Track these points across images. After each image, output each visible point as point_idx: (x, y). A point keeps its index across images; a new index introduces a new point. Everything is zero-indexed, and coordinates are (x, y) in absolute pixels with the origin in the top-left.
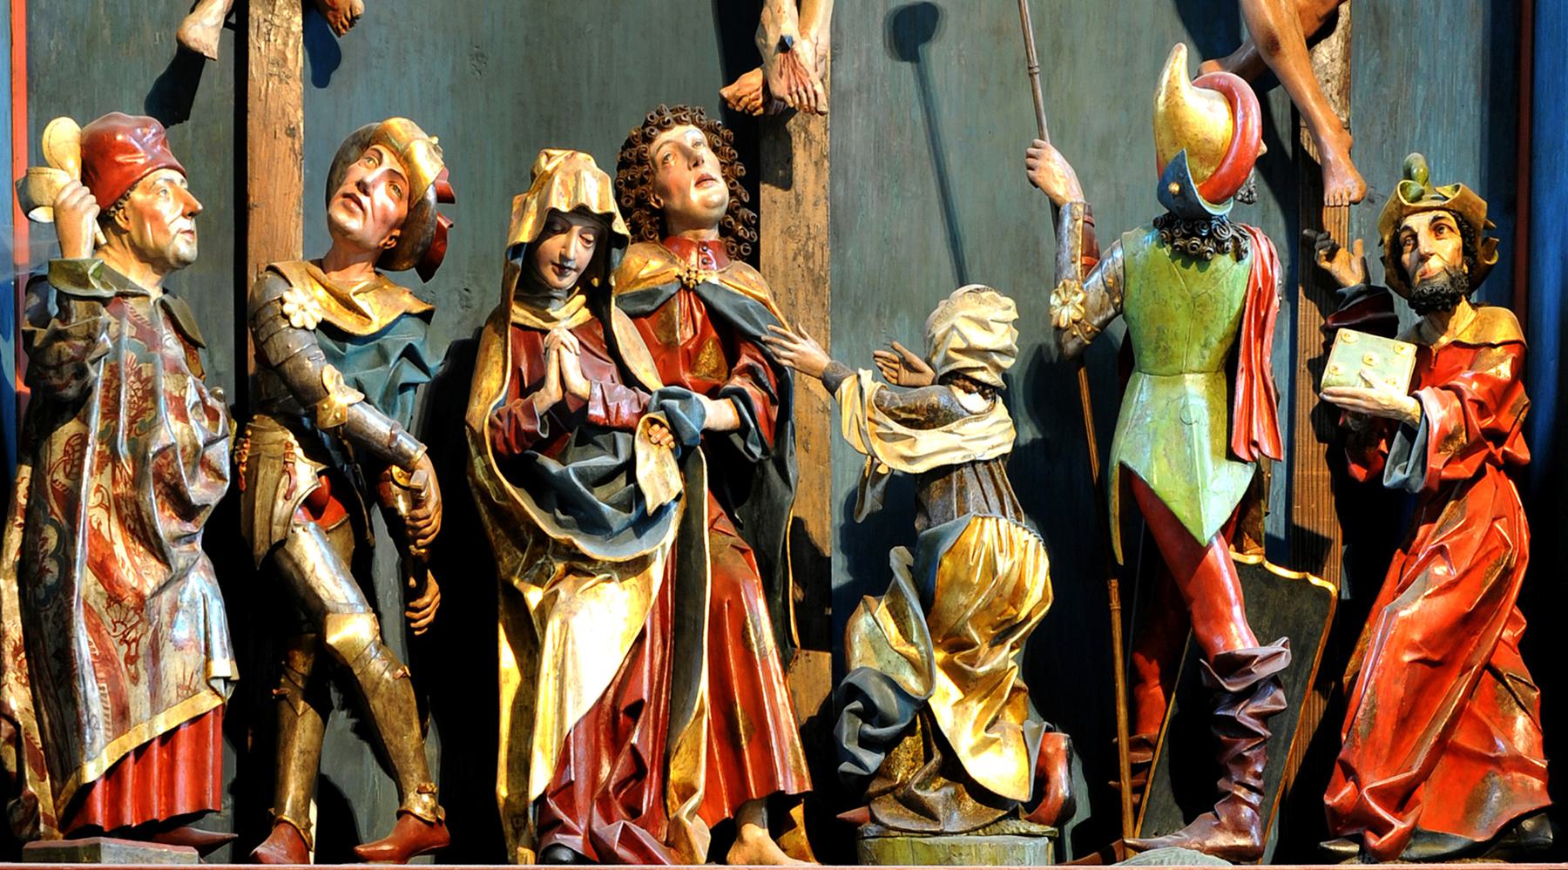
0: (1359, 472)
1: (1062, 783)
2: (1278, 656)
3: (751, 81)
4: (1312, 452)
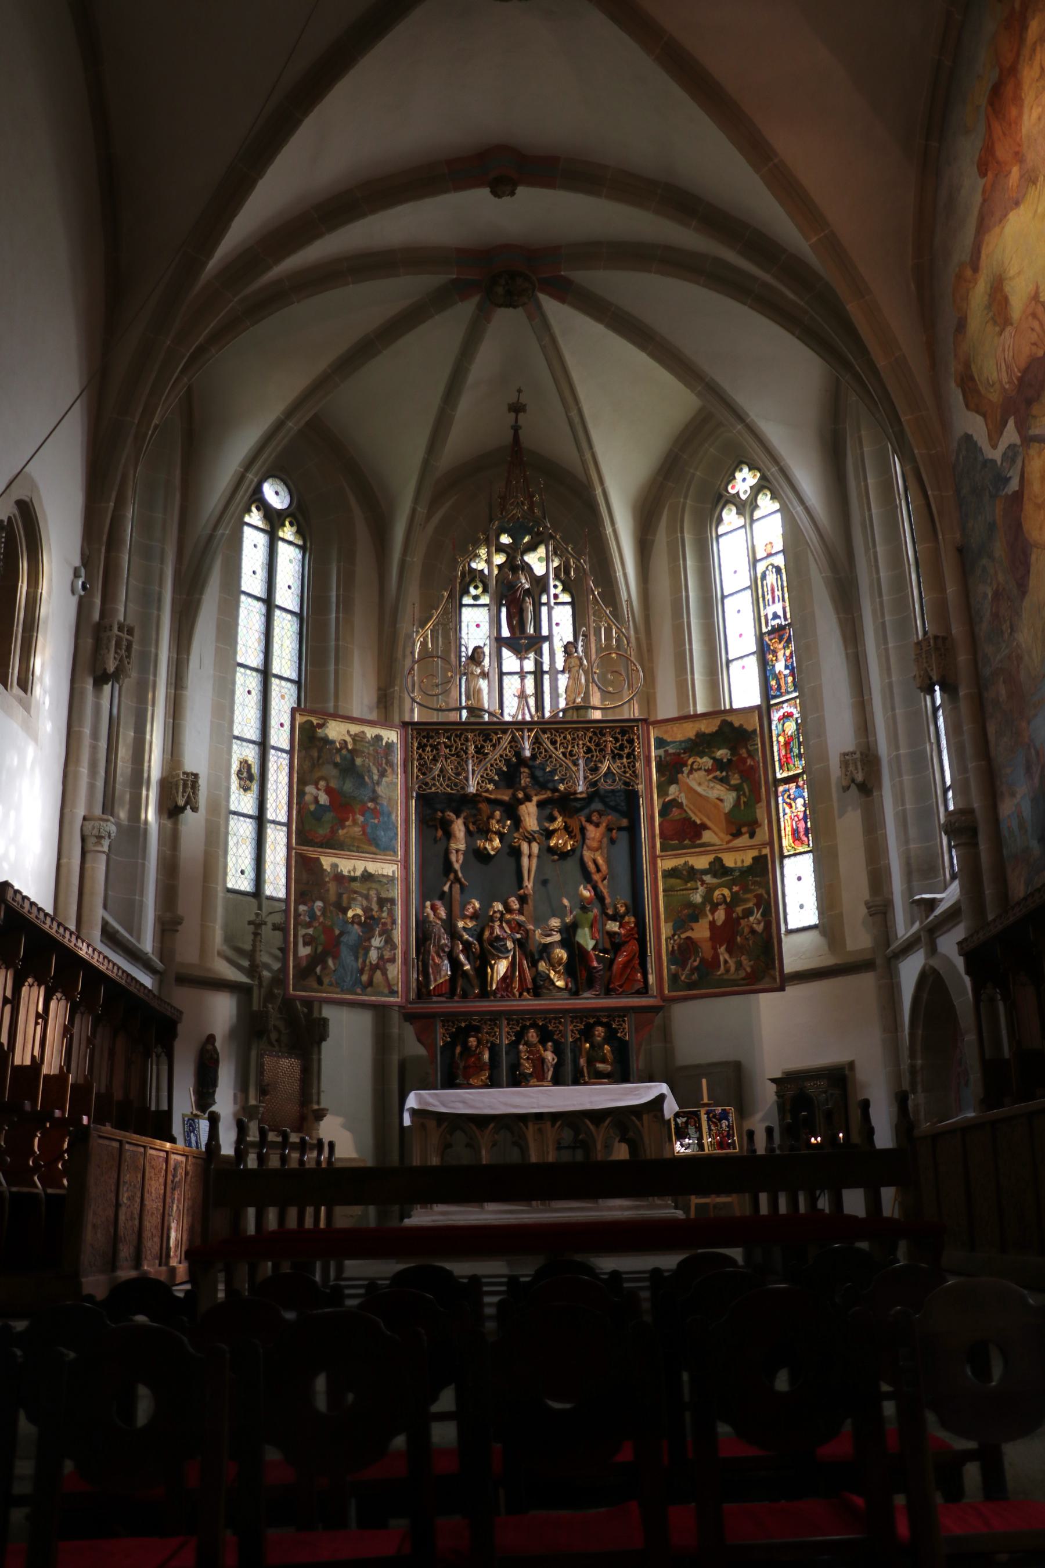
0: (613, 940)
1: (570, 985)
2: (601, 966)
3: (522, 891)
4: (606, 937)
